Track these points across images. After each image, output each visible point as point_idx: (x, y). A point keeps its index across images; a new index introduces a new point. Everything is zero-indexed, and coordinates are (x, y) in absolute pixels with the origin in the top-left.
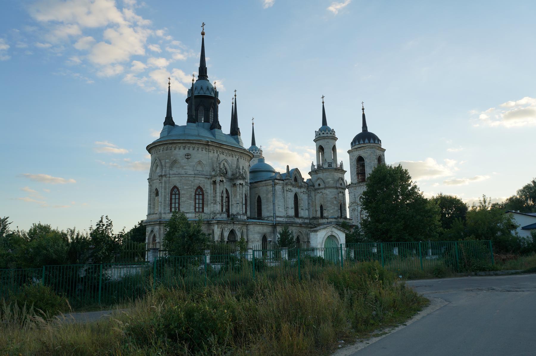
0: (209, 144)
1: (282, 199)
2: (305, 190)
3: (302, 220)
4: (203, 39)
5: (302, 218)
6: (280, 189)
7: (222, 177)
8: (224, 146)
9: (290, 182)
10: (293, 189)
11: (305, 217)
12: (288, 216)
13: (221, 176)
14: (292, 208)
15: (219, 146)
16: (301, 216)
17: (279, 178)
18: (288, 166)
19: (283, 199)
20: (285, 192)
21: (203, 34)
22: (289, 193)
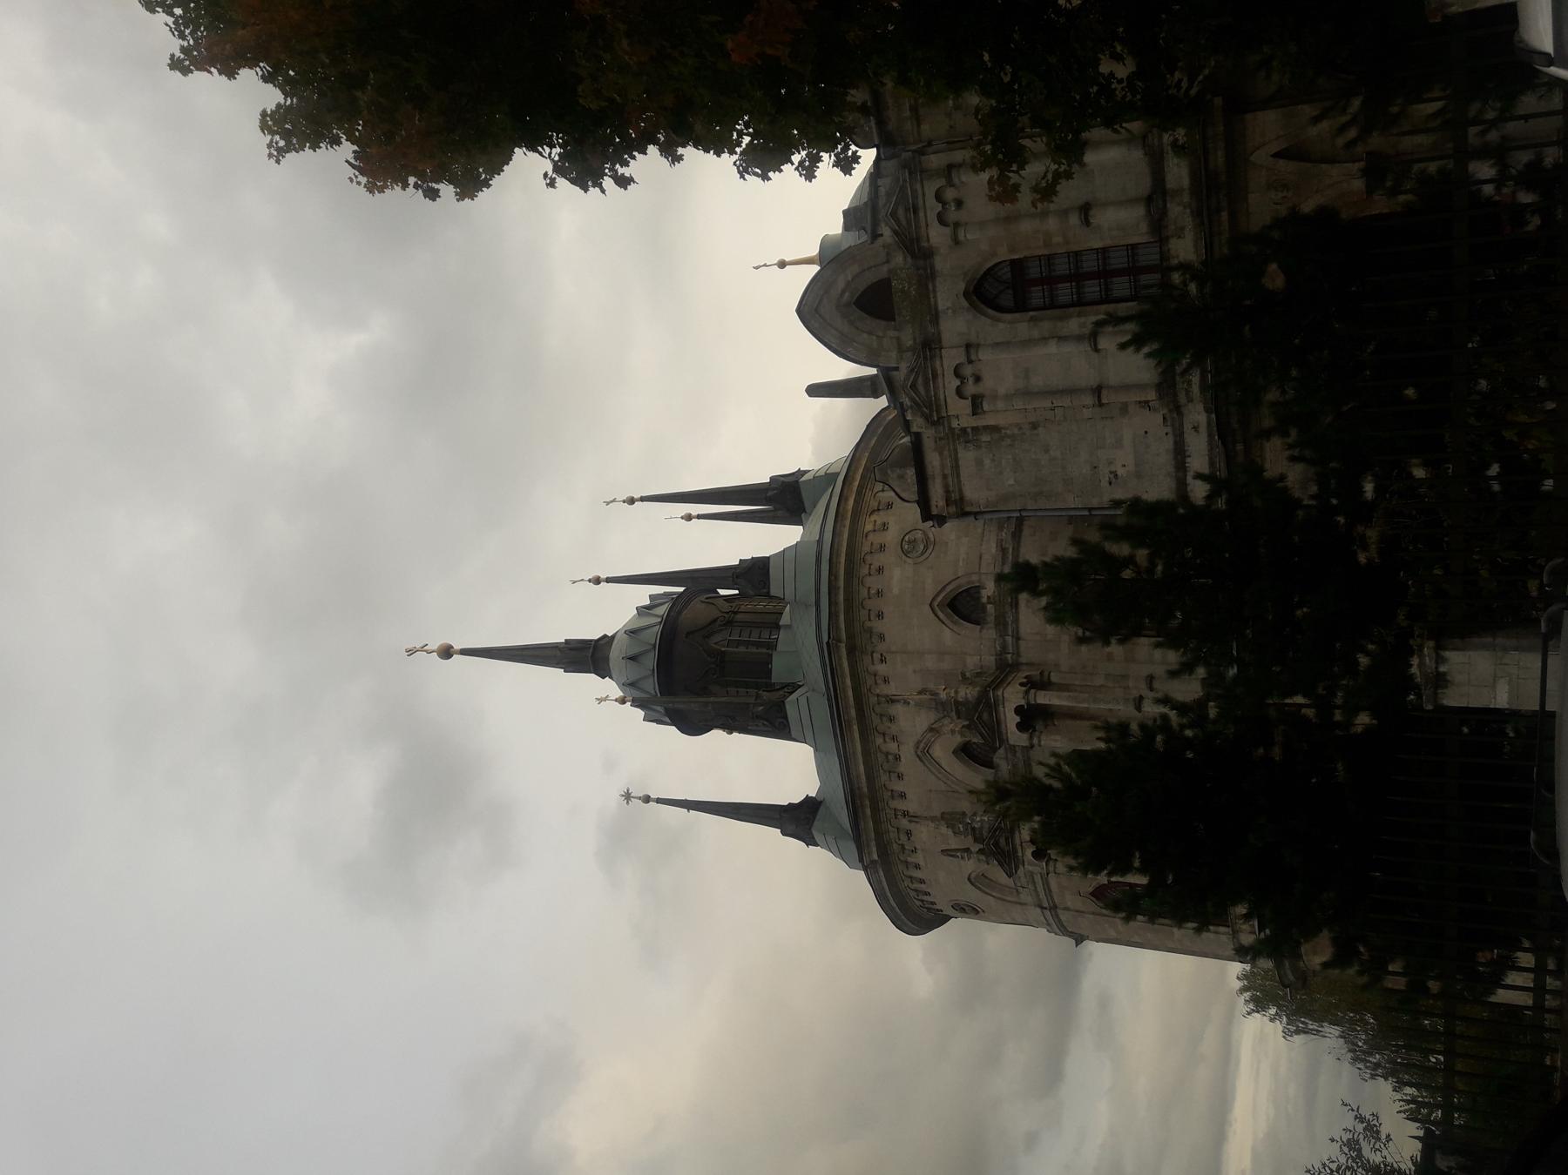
0: (875, 857)
1: (1047, 451)
2: (931, 188)
3: (1180, 233)
4: (466, 652)
5: (1158, 224)
6: (979, 462)
7: (1017, 841)
8: (858, 776)
9: (913, 386)
10: (950, 358)
11: (1144, 185)
12: (1159, 387)
13: (1015, 851)
14: (1097, 350)
15: (867, 802)
16: (1144, 227)
17: (911, 473)
18: (816, 390)
19: (1040, 429)
20: (990, 420)
21: (446, 652)
22: (988, 383)
